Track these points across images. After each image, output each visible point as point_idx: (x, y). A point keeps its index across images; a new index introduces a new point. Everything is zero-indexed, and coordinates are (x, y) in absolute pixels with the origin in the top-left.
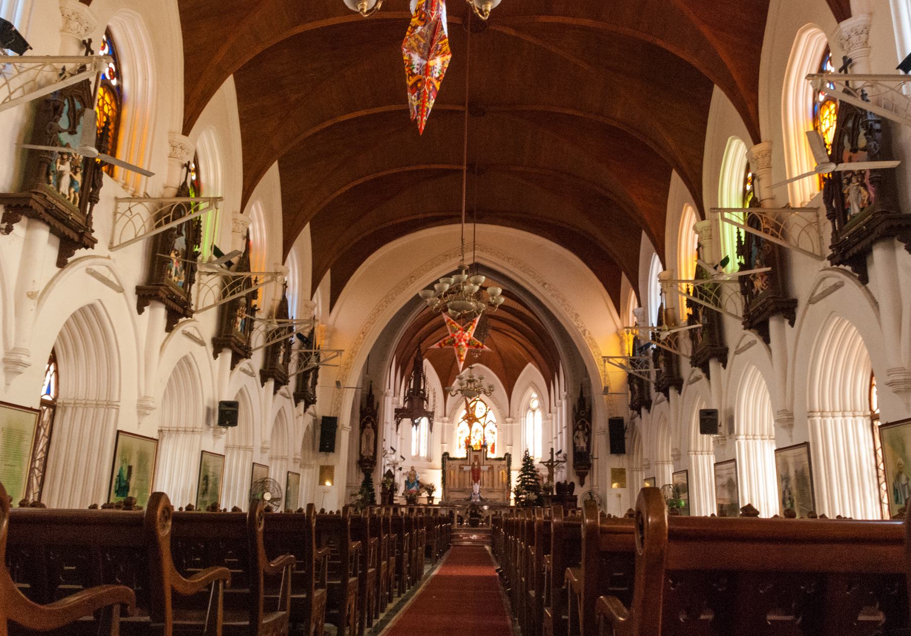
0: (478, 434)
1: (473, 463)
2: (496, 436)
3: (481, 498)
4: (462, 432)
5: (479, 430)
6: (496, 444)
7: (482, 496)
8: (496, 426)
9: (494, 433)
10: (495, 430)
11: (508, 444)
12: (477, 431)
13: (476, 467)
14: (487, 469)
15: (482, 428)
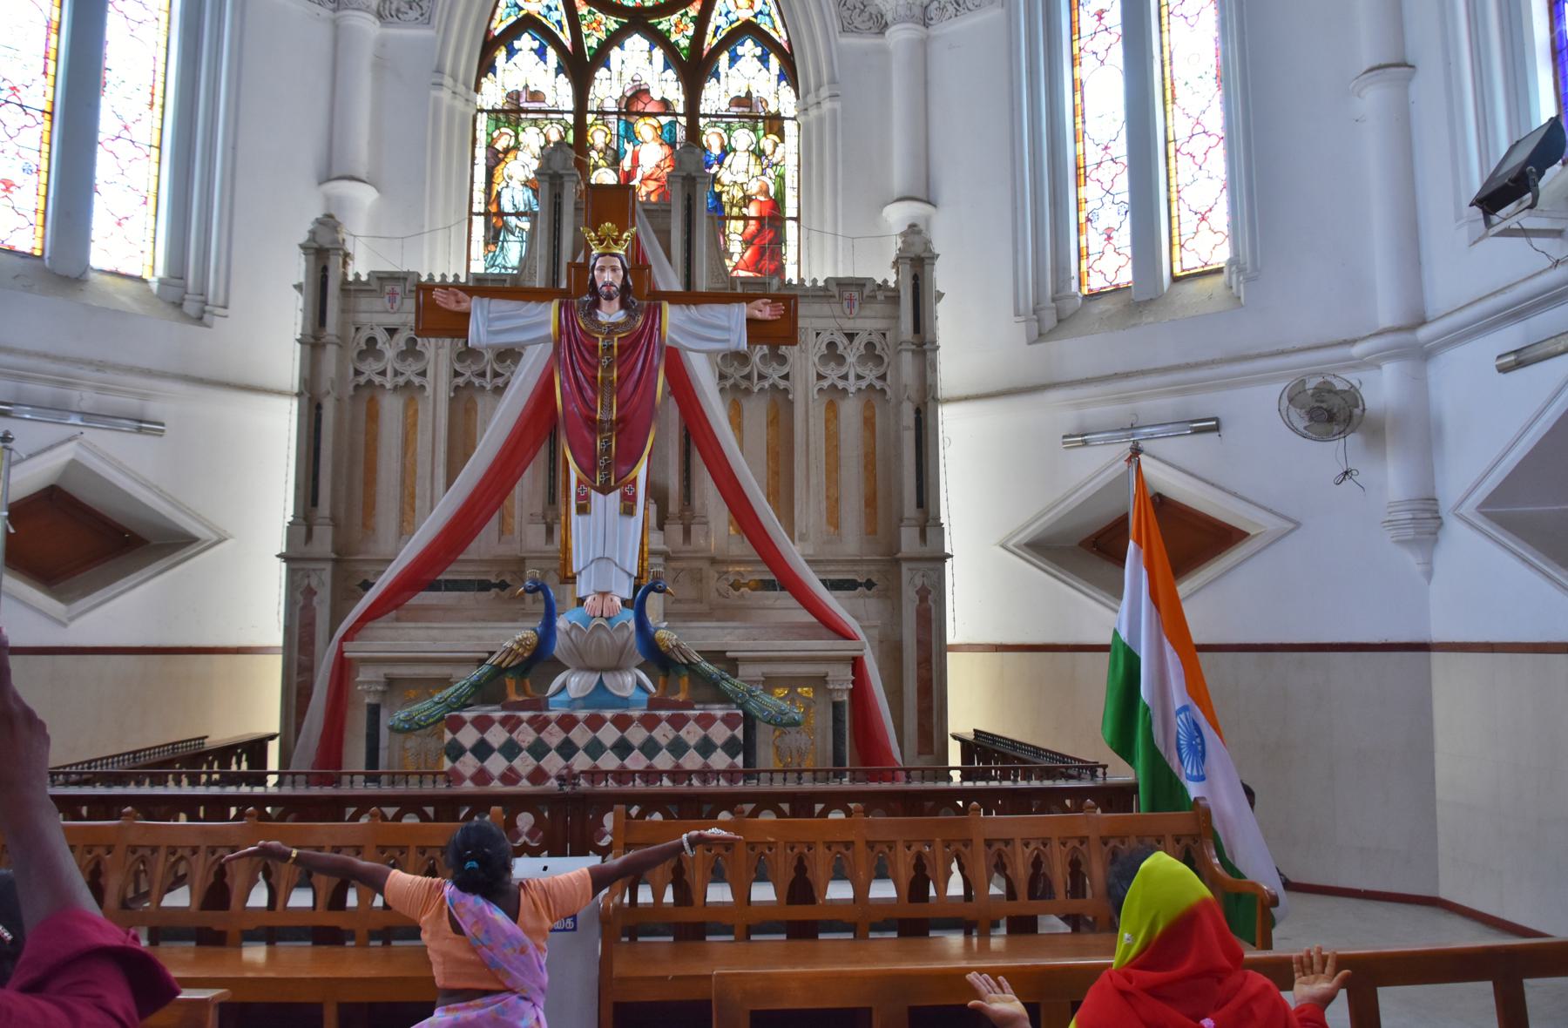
0: (644, 128)
1: (582, 270)
2: (788, 151)
3: (659, 659)
4: (512, 113)
5: (656, 94)
6: (790, 211)
7: (666, 634)
8: (789, 73)
9: (774, 123)
10: (784, 101)
11: (897, 192)
12: (634, 103)
13: (611, 313)
14: (739, 338)
15: (668, 87)
